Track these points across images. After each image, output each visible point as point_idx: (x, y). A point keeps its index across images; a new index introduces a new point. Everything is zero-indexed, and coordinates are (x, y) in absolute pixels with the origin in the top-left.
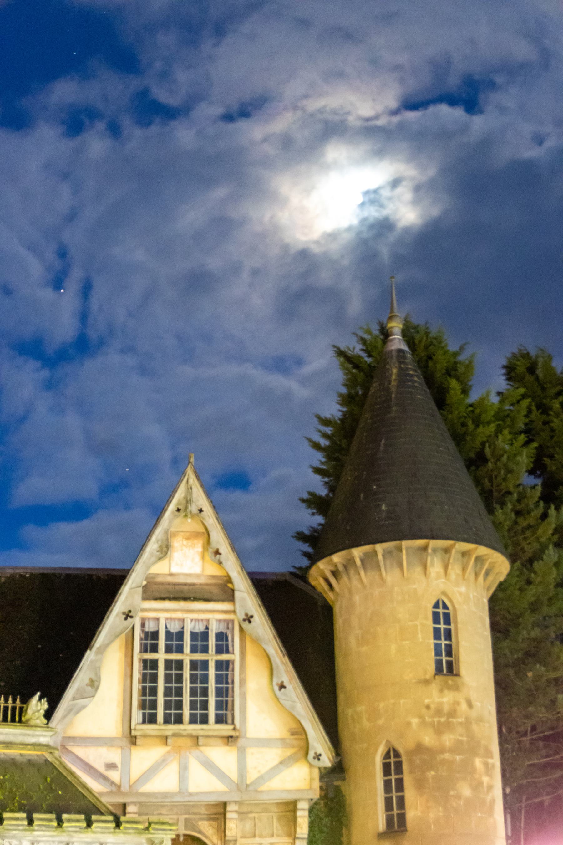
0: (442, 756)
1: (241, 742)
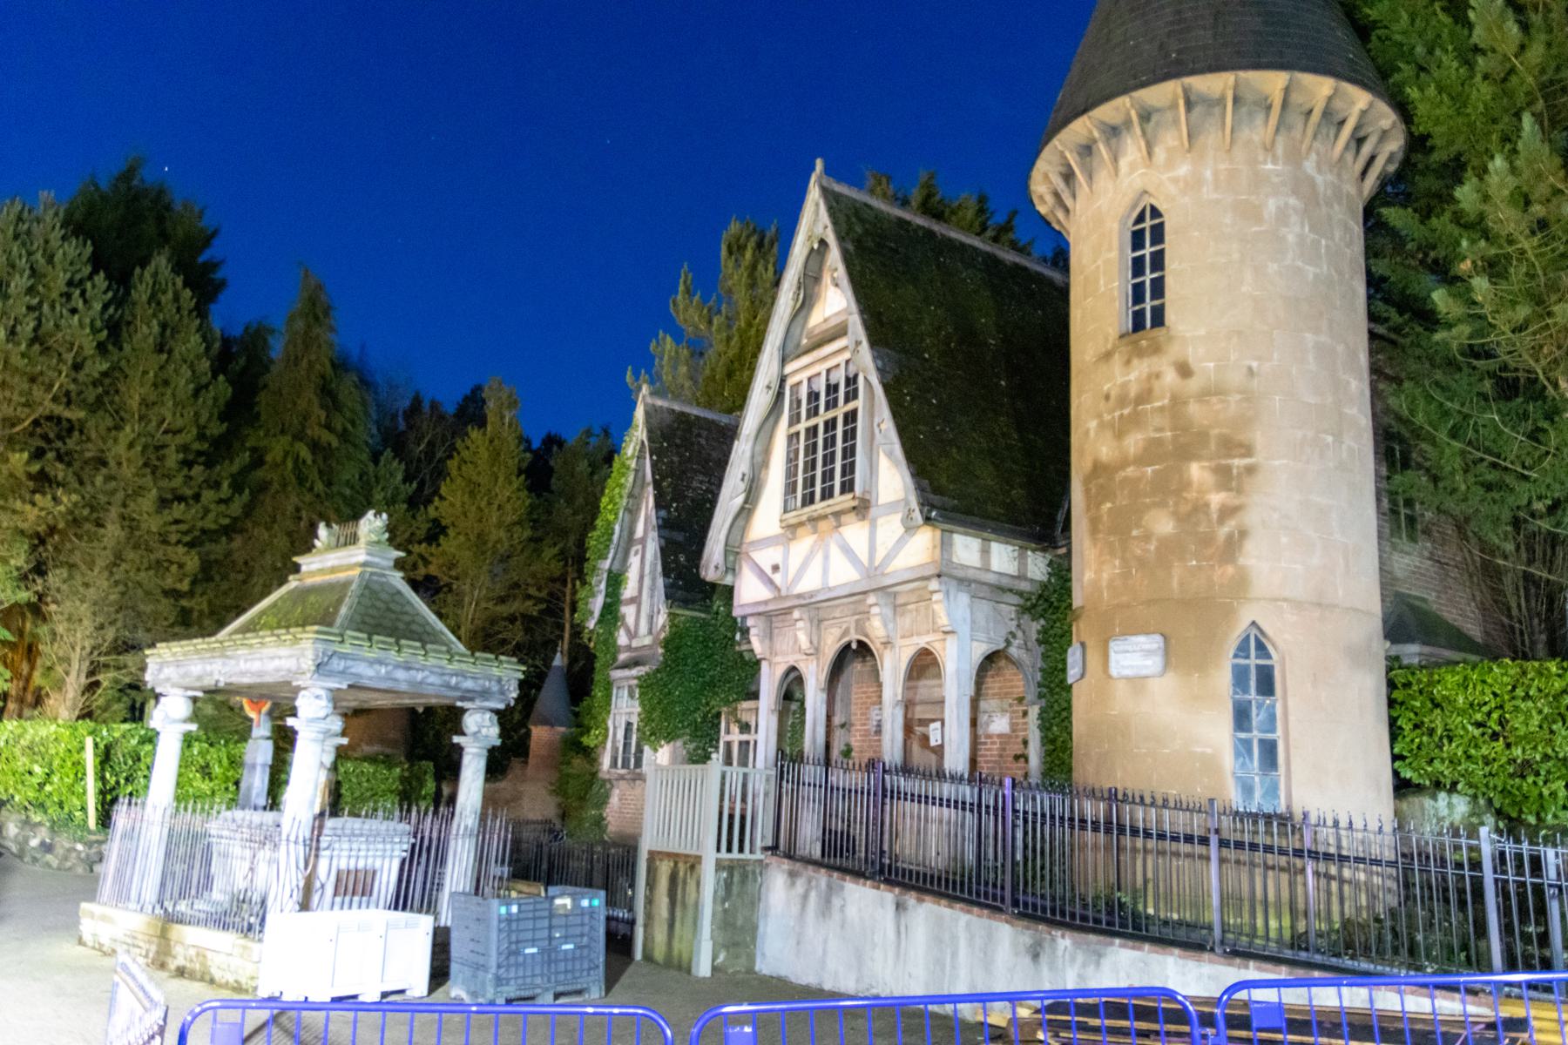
0: (1122, 474)
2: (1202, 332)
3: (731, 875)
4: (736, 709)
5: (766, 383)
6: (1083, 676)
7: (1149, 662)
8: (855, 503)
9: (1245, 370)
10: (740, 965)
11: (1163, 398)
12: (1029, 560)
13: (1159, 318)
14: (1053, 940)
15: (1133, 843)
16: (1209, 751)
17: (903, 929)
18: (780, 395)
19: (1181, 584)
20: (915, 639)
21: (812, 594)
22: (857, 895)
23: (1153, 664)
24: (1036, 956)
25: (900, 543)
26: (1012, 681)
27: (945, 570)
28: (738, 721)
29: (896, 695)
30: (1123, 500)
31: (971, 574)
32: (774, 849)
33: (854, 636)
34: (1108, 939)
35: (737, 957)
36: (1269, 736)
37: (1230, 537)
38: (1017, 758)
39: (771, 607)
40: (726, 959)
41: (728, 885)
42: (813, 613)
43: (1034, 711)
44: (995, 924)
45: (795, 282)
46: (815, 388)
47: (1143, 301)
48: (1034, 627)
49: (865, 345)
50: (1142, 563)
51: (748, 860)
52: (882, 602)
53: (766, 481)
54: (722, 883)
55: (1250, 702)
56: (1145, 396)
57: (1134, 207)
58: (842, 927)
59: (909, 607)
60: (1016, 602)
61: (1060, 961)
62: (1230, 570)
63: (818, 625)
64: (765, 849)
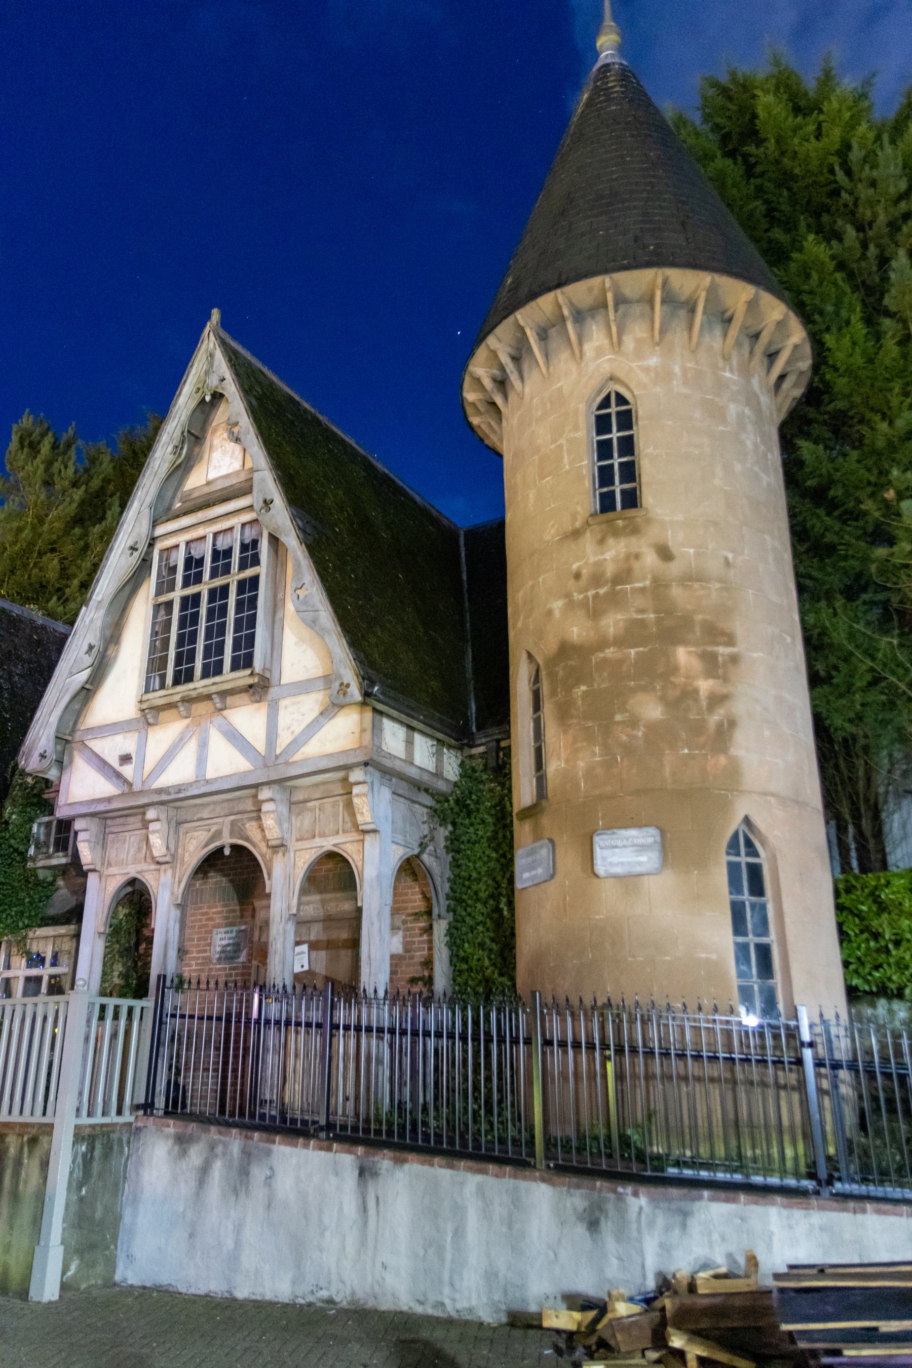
1: (273, 692)
2: (680, 517)
3: (91, 1149)
4: (25, 937)
5: (130, 543)
6: (552, 876)
7: (643, 859)
8: (251, 681)
9: (722, 561)
10: (95, 1279)
11: (644, 579)
12: (445, 757)
13: (632, 500)
14: (620, 1198)
15: (633, 1064)
16: (714, 957)
17: (371, 1203)
18: (145, 562)
19: (674, 774)
20: (318, 842)
21: (179, 788)
22: (294, 1161)
23: (648, 860)
24: (593, 1225)
25: (312, 728)
26: (406, 894)
27: (375, 757)
28: (28, 954)
29: (289, 908)
30: (602, 683)
31: (398, 766)
32: (147, 1107)
33: (227, 840)
34: (694, 1192)
35: (92, 1264)
36: (763, 940)
37: (720, 725)
38: (413, 981)
39: (116, 805)
40: (79, 1268)
41: (87, 1161)
42: (172, 813)
43: (441, 928)
44: (523, 1184)
45: (178, 432)
46: (196, 554)
47: (612, 483)
48: (443, 833)
49: (279, 502)
50: (628, 750)
51: (114, 1125)
52: (278, 797)
53: (116, 658)
54: (79, 1159)
55: (743, 903)
56: (624, 576)
57: (600, 391)
58: (269, 1206)
59: (310, 804)
60: (429, 804)
61: (634, 1226)
62: (723, 760)
63: (177, 831)
64: (136, 1107)
